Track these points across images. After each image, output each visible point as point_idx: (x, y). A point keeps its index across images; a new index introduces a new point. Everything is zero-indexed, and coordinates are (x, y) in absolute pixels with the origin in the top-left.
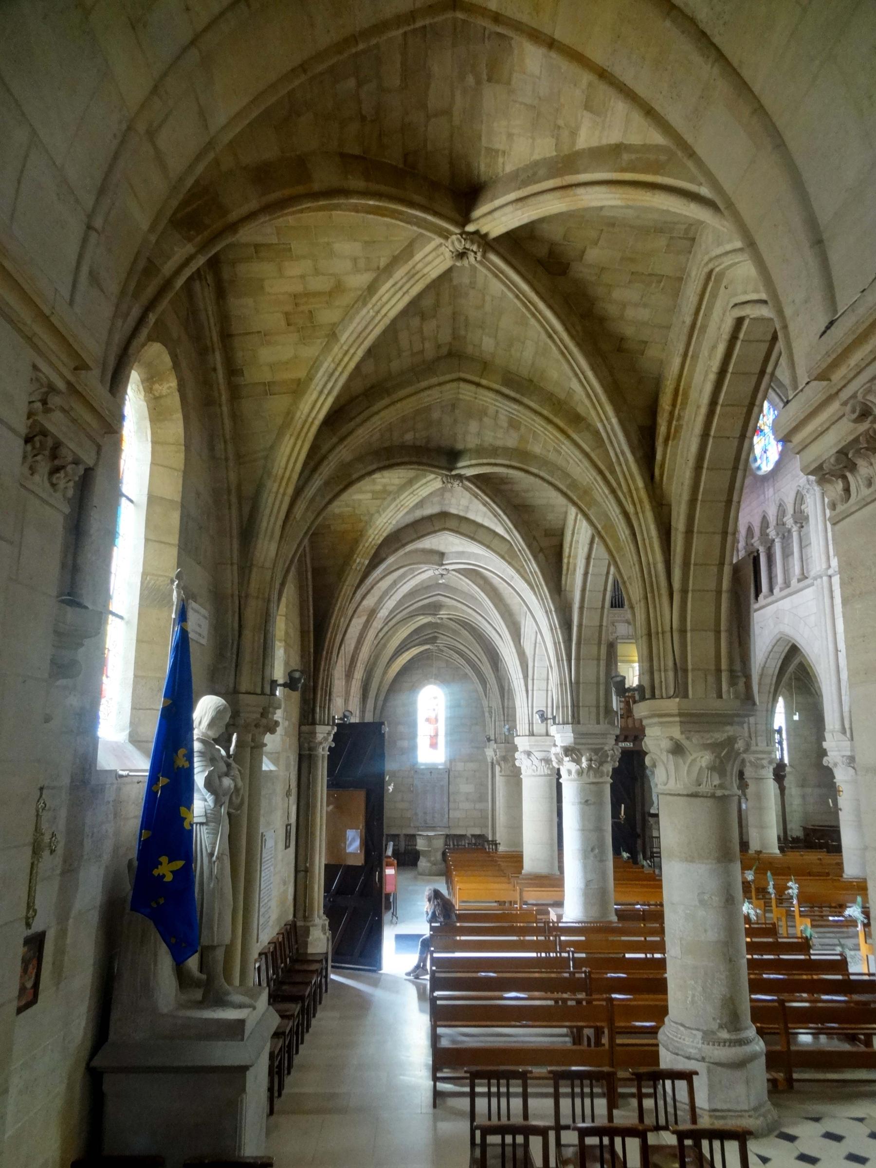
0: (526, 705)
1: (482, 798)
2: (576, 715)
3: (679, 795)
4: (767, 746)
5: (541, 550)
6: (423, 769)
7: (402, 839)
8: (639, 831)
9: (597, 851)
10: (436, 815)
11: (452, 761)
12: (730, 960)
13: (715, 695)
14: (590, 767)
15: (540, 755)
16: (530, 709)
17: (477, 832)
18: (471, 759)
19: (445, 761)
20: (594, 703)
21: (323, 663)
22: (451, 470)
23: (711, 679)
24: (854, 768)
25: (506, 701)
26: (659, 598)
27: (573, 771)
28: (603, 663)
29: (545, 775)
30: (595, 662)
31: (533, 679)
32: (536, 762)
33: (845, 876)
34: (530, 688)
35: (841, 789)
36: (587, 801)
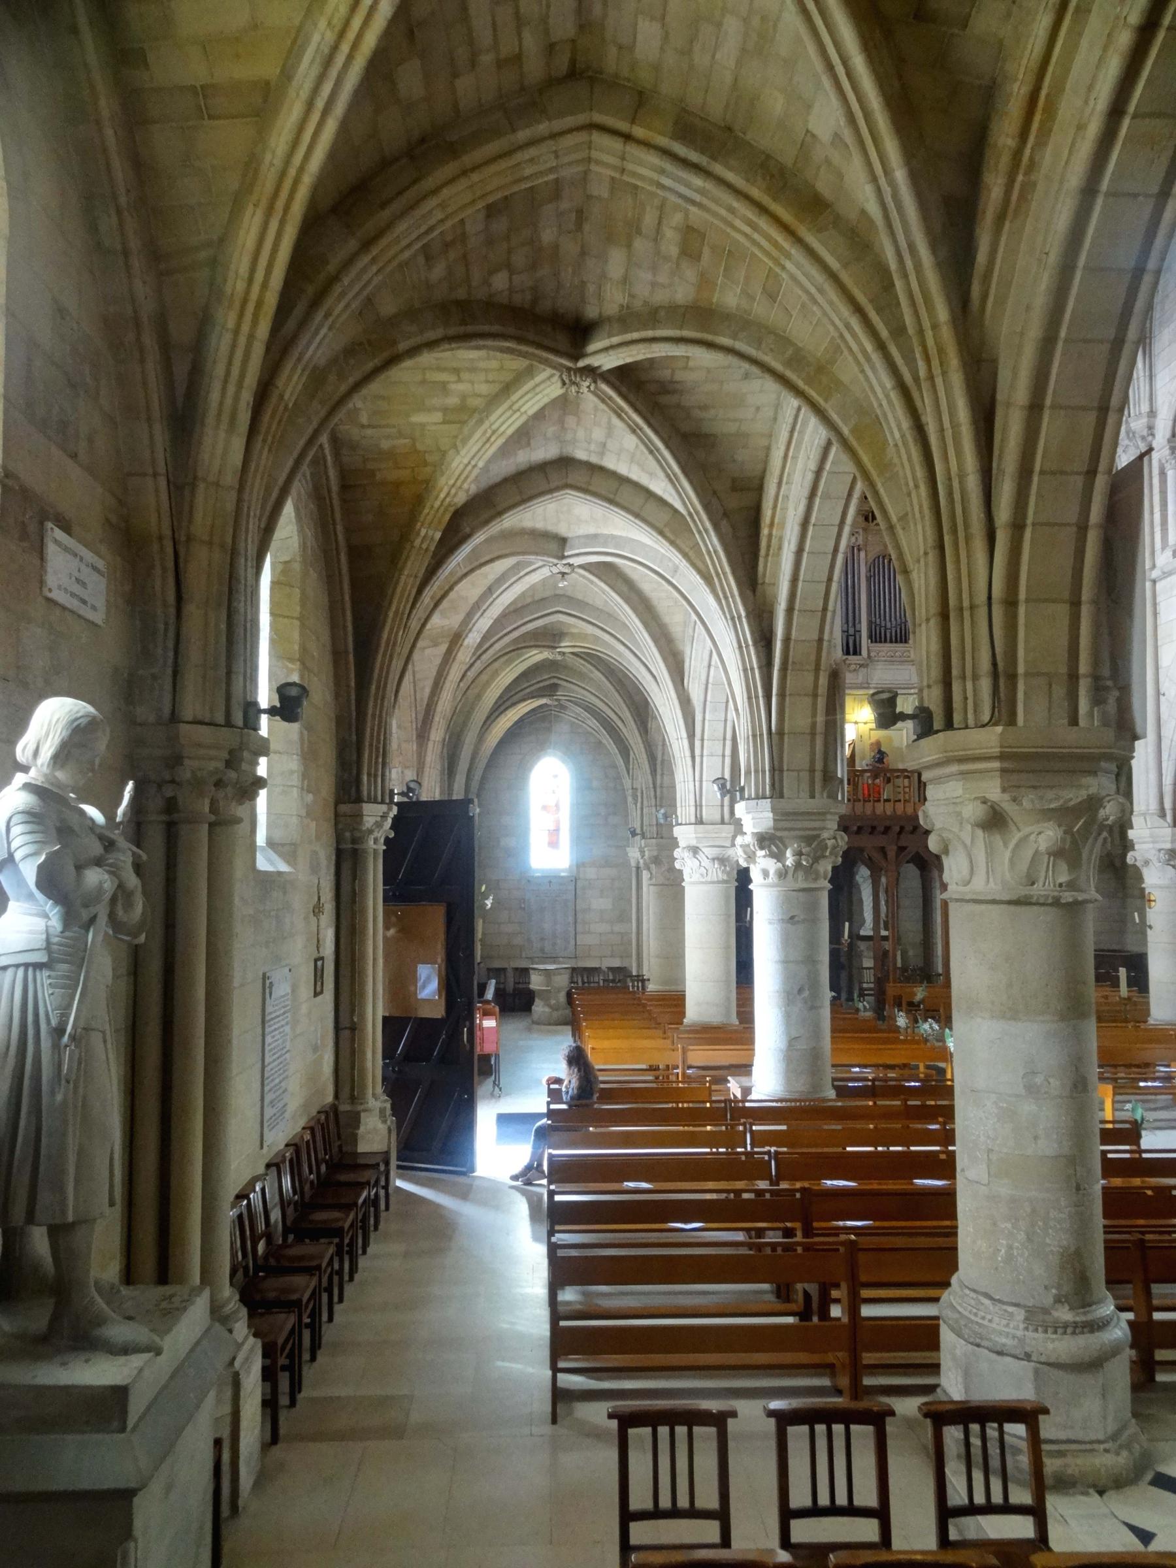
0: (691, 779)
1: (623, 917)
2: (777, 785)
3: (994, 902)
5: (725, 514)
7: (510, 974)
9: (806, 993)
11: (580, 866)
12: (1078, 1188)
13: (1065, 721)
14: (798, 865)
16: (697, 784)
17: (616, 963)
18: (607, 863)
20: (807, 766)
21: (371, 704)
22: (576, 358)
23: (1059, 691)
25: (659, 777)
26: (967, 543)
27: (772, 872)
28: (821, 702)
29: (719, 882)
30: (808, 701)
31: (702, 740)
32: (706, 863)
33: (1151, 1021)
34: (697, 752)
35: (1152, 898)
36: (792, 918)
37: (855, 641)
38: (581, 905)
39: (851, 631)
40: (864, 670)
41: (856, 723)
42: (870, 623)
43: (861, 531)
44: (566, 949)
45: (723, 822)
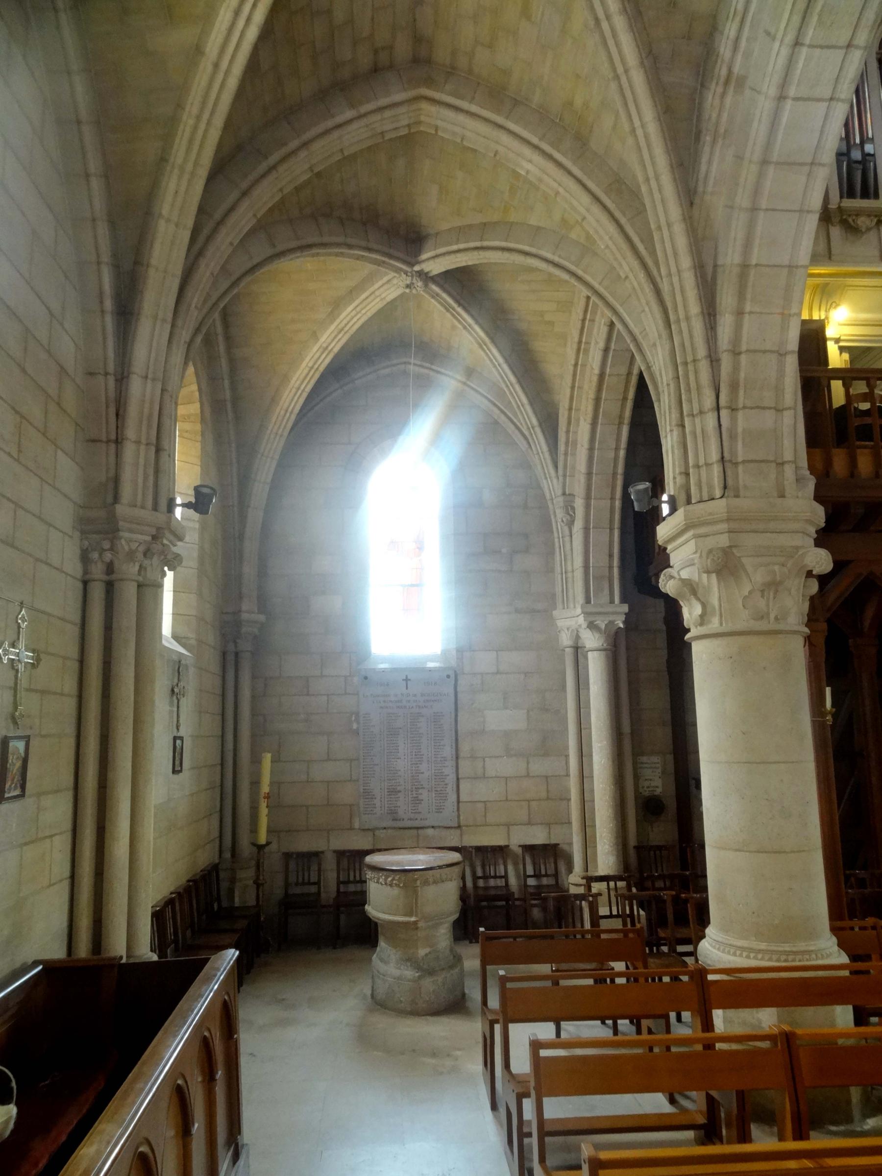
6: (384, 671)
7: (330, 864)
10: (424, 795)
17: (538, 837)
19: (445, 653)
38: (466, 723)
44: (439, 810)
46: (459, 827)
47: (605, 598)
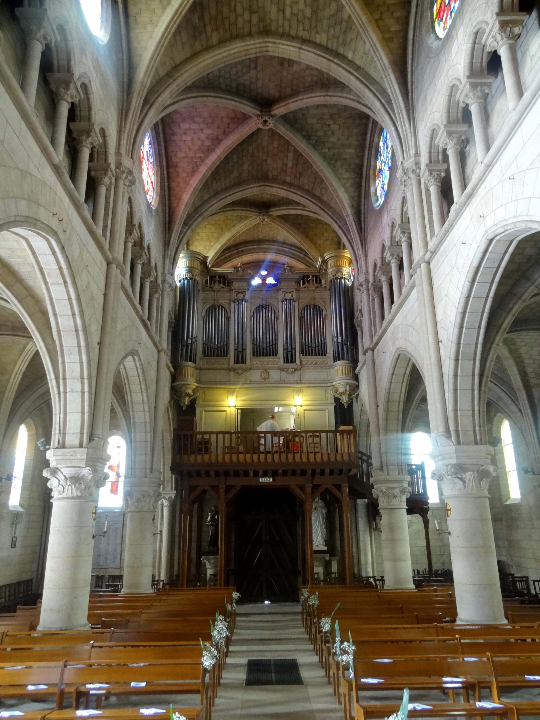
4: (399, 474)
8: (300, 567)
10: (109, 556)
15: (67, 472)
24: (461, 479)
29: (73, 498)
31: (64, 379)
35: (449, 508)
37: (292, 354)
39: (289, 349)
40: (297, 373)
41: (295, 406)
42: (302, 344)
43: (294, 290)
44: (114, 562)
45: (81, 446)
46: (120, 568)
47: (170, 488)
